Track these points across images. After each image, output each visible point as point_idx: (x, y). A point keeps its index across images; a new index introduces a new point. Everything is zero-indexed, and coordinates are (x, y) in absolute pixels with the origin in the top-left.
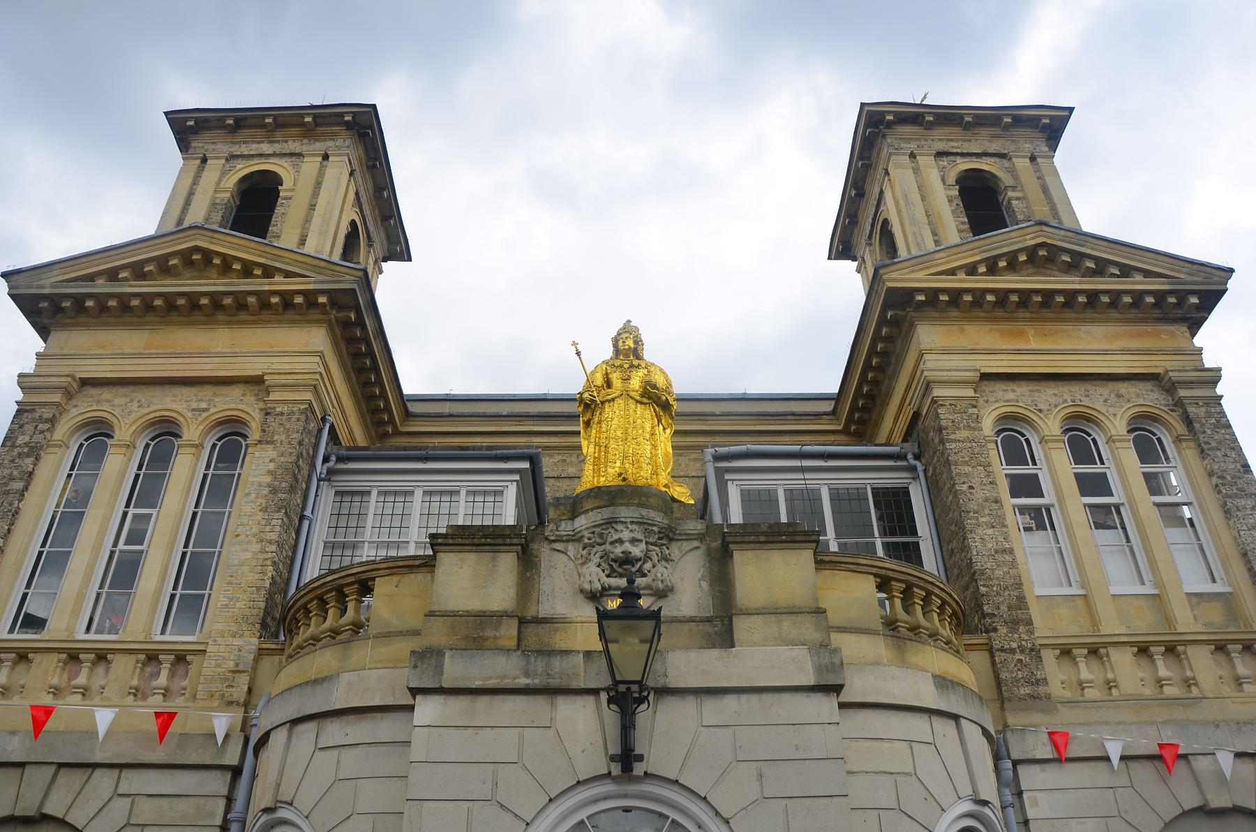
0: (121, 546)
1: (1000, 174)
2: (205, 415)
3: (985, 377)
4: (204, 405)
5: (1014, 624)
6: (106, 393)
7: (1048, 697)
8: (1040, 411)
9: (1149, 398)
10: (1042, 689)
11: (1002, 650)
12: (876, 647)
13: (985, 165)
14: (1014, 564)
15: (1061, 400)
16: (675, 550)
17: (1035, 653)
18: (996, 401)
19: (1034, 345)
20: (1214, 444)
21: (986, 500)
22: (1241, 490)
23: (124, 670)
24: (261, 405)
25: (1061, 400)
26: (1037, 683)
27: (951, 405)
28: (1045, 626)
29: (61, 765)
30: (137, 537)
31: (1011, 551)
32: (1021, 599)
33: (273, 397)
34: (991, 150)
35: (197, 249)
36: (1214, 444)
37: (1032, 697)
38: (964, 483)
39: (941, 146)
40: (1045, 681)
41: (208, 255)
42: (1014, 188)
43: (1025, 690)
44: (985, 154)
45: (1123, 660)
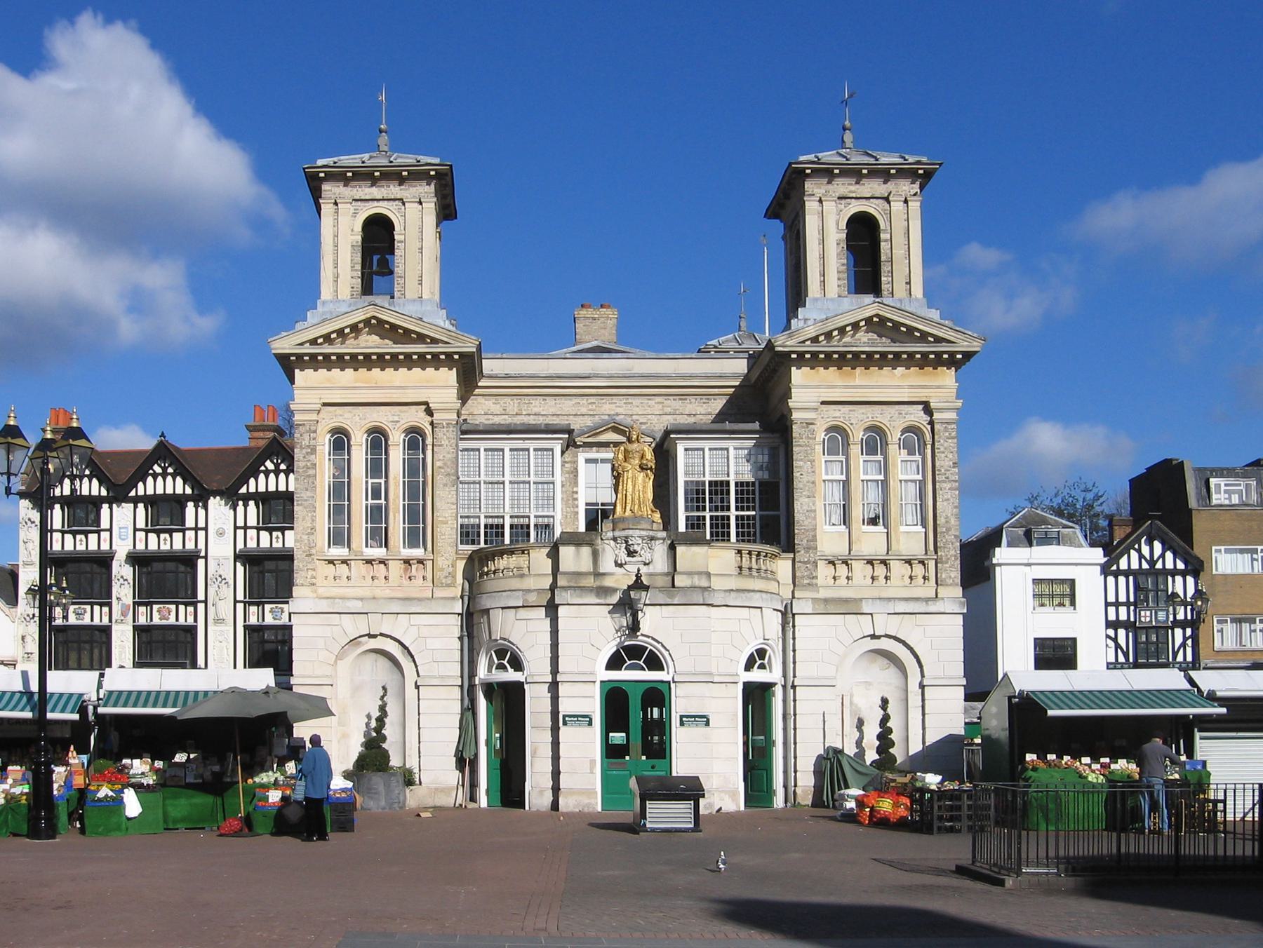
2: (398, 425)
4: (396, 418)
5: (808, 549)
7: (816, 585)
8: (851, 424)
10: (814, 581)
14: (815, 518)
15: (865, 416)
17: (815, 563)
18: (828, 418)
19: (857, 382)
21: (808, 482)
22: (947, 478)
23: (396, 568)
24: (429, 419)
25: (865, 416)
26: (813, 578)
27: (801, 423)
31: (815, 511)
32: (815, 536)
35: (374, 317)
37: (809, 584)
38: (798, 472)
40: (817, 577)
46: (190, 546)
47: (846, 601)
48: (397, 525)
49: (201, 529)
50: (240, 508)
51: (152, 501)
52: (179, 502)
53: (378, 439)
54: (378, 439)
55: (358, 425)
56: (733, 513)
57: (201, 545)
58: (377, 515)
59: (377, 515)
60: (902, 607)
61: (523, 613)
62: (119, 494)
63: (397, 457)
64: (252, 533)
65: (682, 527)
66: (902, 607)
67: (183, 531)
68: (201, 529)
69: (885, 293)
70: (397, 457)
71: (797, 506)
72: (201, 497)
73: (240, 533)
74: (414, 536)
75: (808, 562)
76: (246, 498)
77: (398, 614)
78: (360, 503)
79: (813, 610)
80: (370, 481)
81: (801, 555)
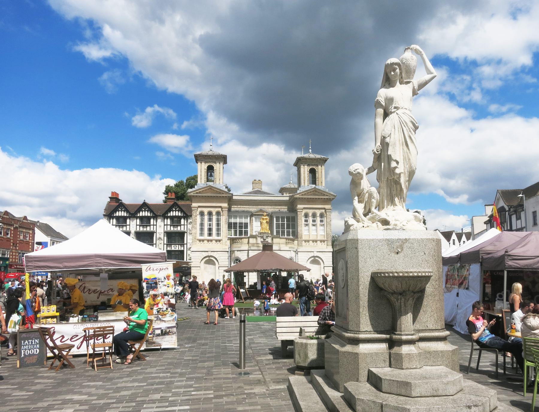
5: (301, 238)
12: (284, 245)
16: (269, 237)
28: (304, 238)
33: (223, 209)
39: (308, 163)
42: (317, 172)
45: (311, 242)
46: (152, 229)
48: (214, 232)
49: (155, 225)
50: (166, 220)
51: (142, 218)
52: (149, 218)
53: (210, 214)
54: (210, 214)
56: (286, 230)
57: (155, 230)
58: (210, 230)
59: (210, 230)
62: (133, 216)
63: (214, 218)
64: (169, 227)
65: (275, 234)
67: (150, 226)
68: (155, 225)
69: (317, 185)
70: (214, 218)
72: (155, 217)
73: (166, 226)
74: (218, 234)
76: (167, 218)
78: (206, 227)
80: (209, 223)
81: (299, 239)
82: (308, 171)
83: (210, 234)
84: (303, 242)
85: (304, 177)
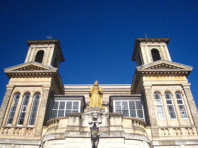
0: (22, 111)
1: (158, 49)
3: (153, 85)
4: (34, 90)
5: (155, 125)
6: (19, 88)
7: (159, 136)
9: (179, 88)
10: (158, 135)
11: (153, 129)
13: (156, 48)
14: (155, 115)
17: (158, 129)
20: (188, 96)
22: (192, 103)
29: (16, 144)
30: (24, 110)
31: (155, 113)
32: (156, 121)
33: (44, 89)
34: (157, 45)
36: (188, 96)
41: (34, 66)
42: (160, 52)
43: (155, 135)
44: (156, 46)
47: (170, 141)
54: (27, 94)
55: (22, 91)
60: (188, 143)
61: (54, 142)
63: (31, 100)
66: (188, 143)
71: (149, 112)
75: (155, 129)
77: (20, 144)
79: (159, 144)
80: (24, 106)
81: (153, 127)
82: (150, 51)
83: (21, 122)
84: (160, 129)
85: (146, 57)
